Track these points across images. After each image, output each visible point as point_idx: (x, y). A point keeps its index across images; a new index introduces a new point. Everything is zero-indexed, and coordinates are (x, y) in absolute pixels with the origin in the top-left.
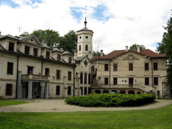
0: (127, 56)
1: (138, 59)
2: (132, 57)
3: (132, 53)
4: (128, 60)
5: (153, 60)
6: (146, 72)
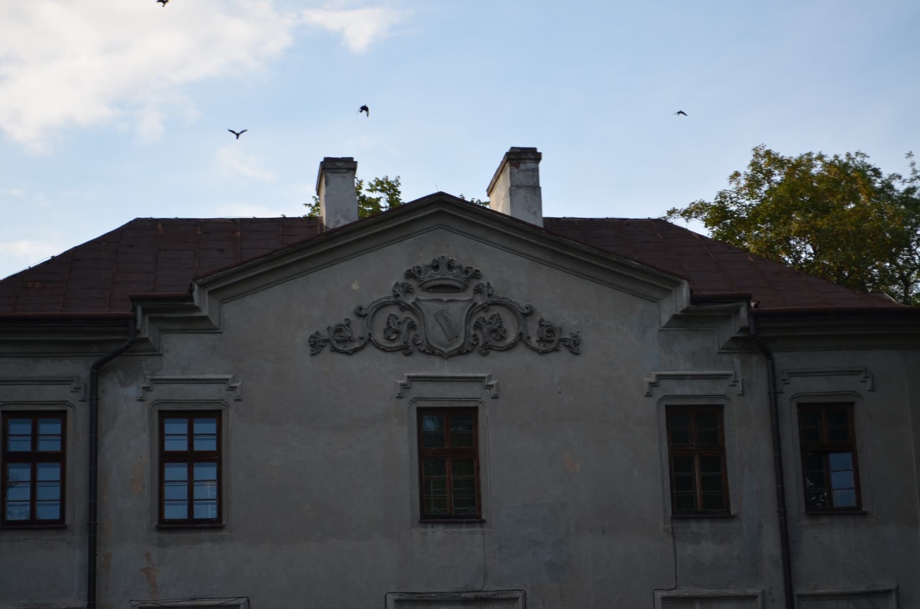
0: (386, 293)
1: (553, 340)
2: (457, 307)
3: (459, 248)
4: (406, 350)
5: (784, 360)
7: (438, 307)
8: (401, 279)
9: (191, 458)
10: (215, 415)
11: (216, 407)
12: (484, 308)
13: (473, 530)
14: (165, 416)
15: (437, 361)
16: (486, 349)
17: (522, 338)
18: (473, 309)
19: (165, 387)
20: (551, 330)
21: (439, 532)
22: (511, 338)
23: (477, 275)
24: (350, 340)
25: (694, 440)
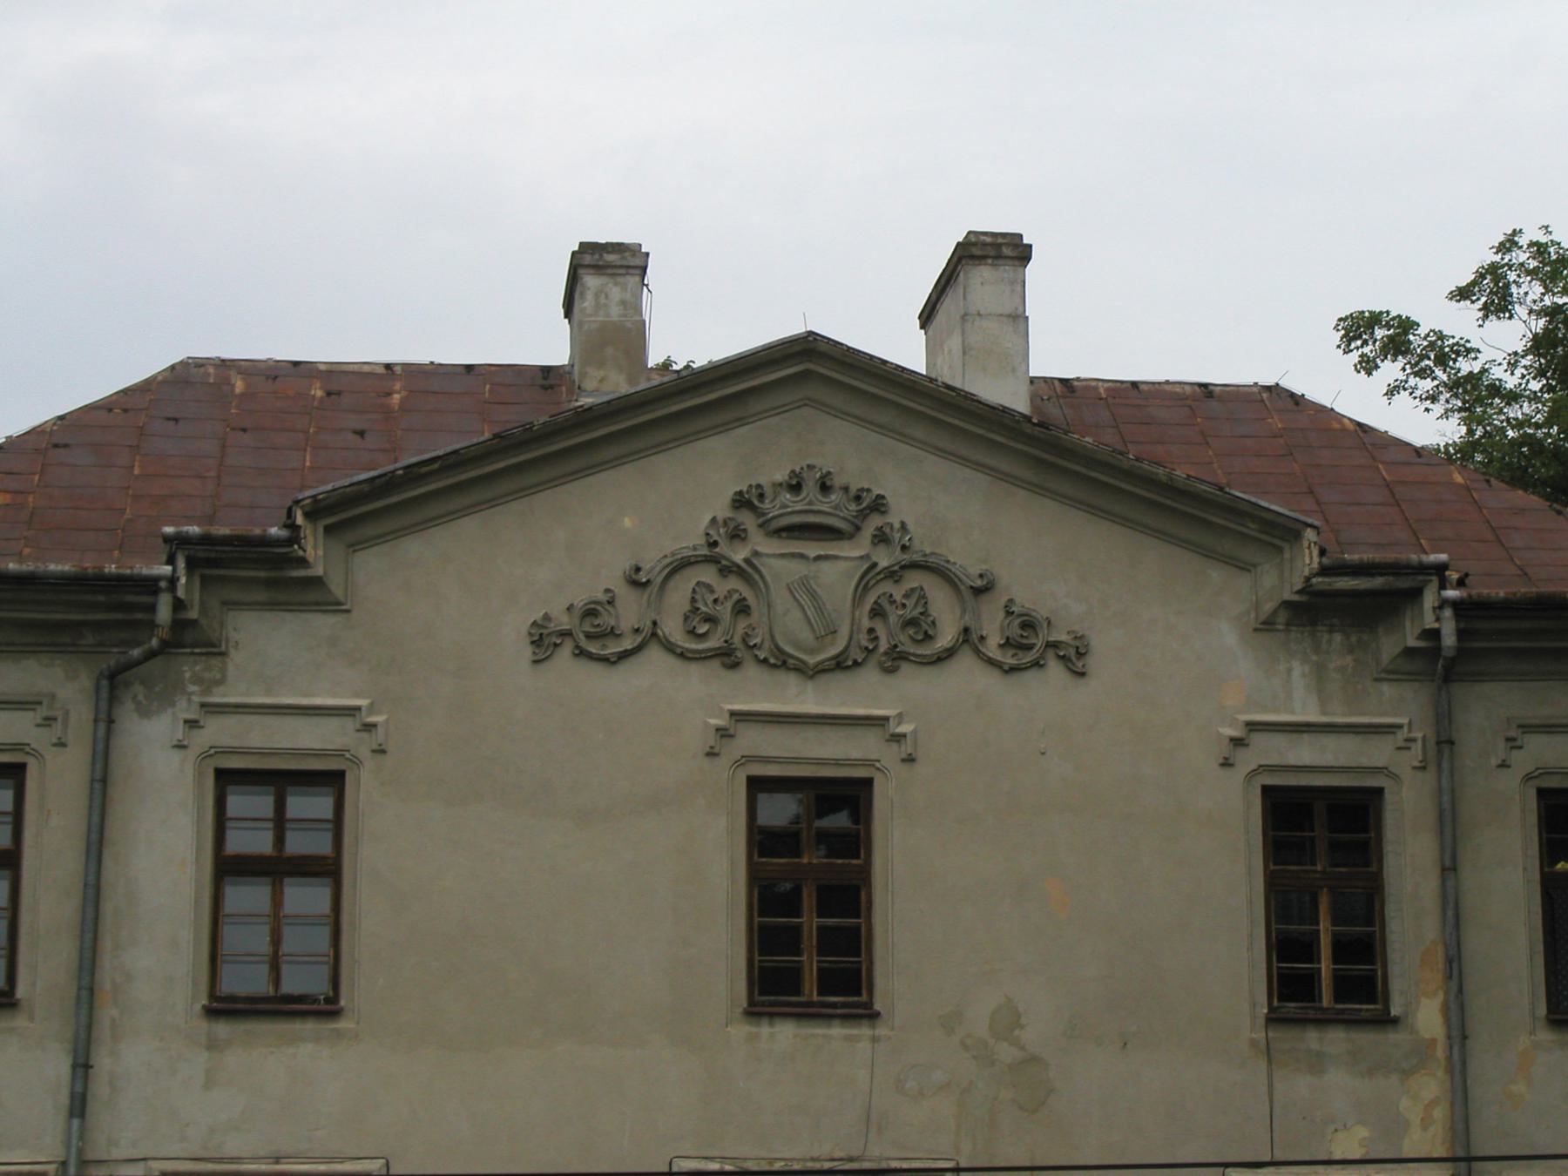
0: (691, 539)
1: (1030, 645)
2: (836, 571)
3: (847, 450)
4: (728, 658)
6: (1297, 1086)
7: (796, 569)
8: (722, 510)
9: (277, 868)
10: (333, 781)
11: (333, 765)
12: (893, 575)
13: (855, 1032)
14: (227, 779)
15: (792, 681)
16: (895, 660)
17: (968, 638)
18: (870, 575)
19: (231, 722)
20: (1029, 625)
21: (784, 1034)
22: (946, 637)
23: (878, 505)
24: (612, 633)
25: (1318, 840)
